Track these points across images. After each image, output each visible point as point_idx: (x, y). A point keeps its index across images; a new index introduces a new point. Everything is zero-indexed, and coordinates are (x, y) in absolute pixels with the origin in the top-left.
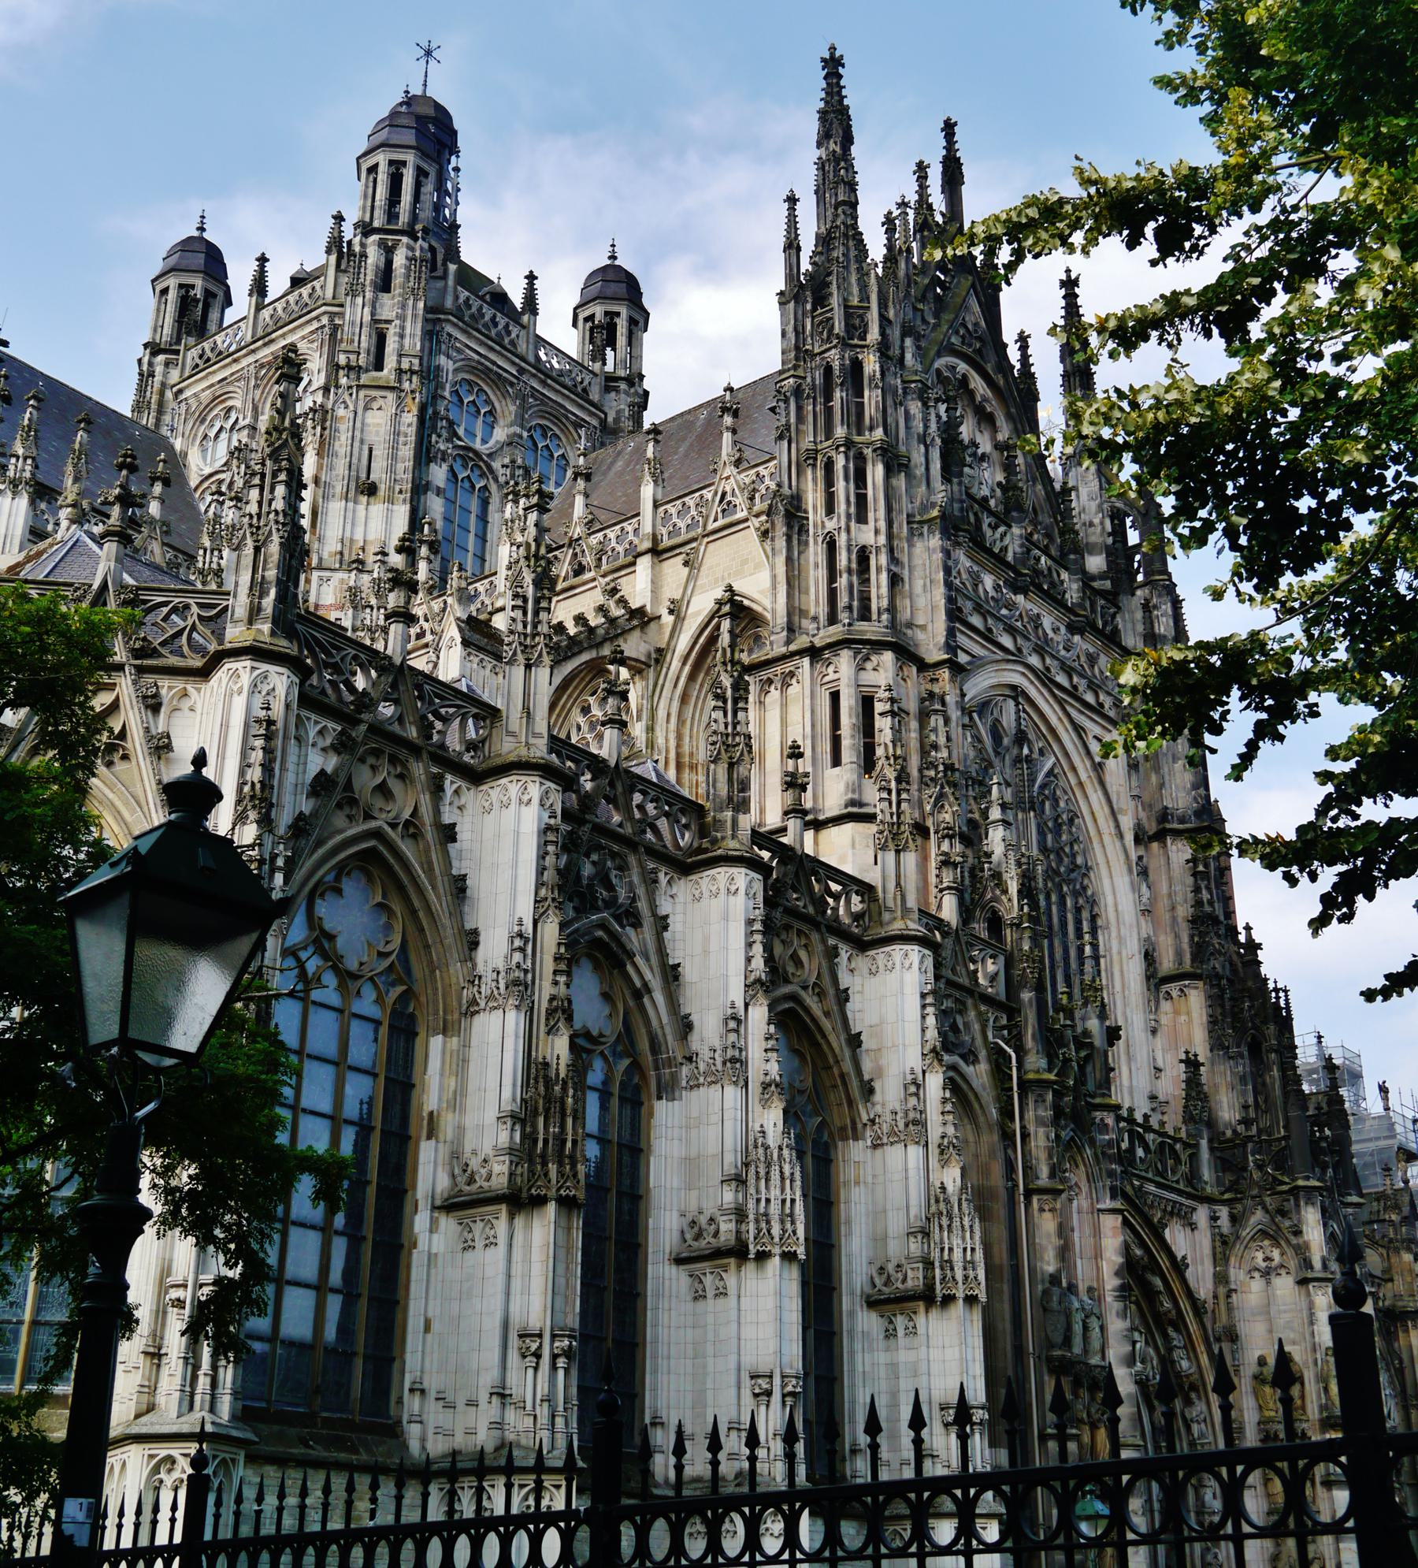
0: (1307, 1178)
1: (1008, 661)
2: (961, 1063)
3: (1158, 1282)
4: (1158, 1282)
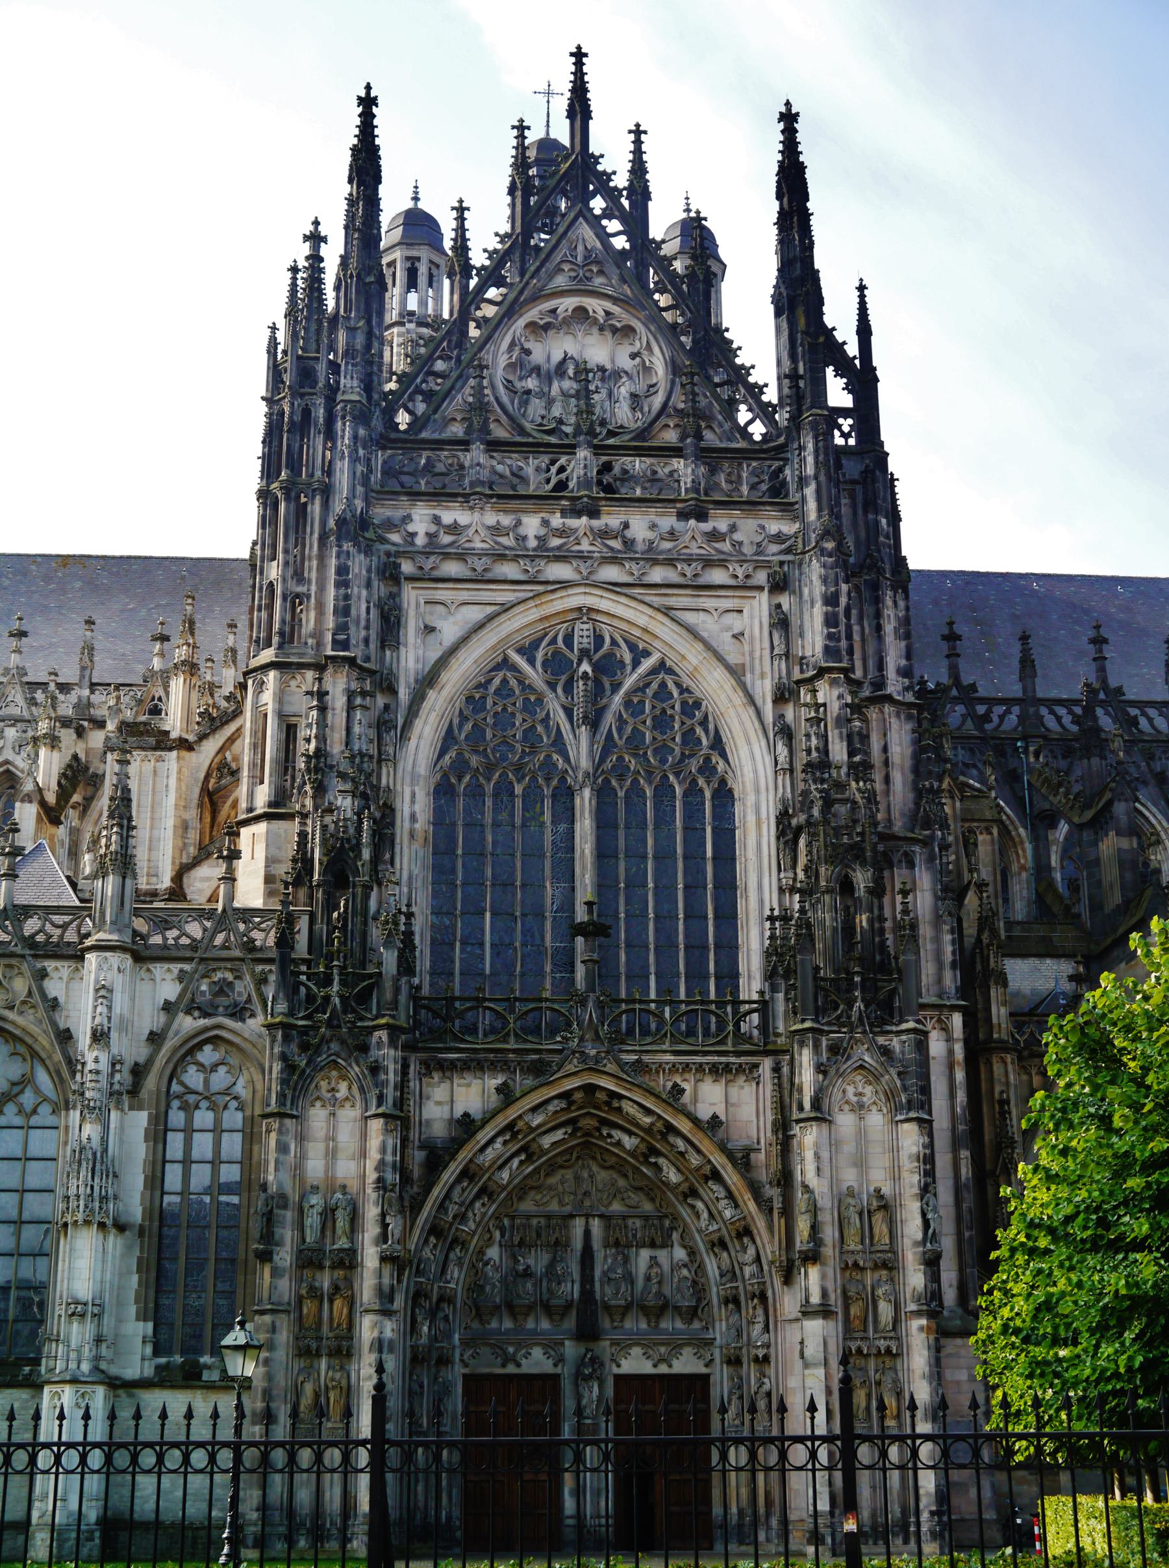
0: (803, 1021)
1: (553, 591)
2: (228, 1022)
3: (681, 1144)
4: (681, 1144)
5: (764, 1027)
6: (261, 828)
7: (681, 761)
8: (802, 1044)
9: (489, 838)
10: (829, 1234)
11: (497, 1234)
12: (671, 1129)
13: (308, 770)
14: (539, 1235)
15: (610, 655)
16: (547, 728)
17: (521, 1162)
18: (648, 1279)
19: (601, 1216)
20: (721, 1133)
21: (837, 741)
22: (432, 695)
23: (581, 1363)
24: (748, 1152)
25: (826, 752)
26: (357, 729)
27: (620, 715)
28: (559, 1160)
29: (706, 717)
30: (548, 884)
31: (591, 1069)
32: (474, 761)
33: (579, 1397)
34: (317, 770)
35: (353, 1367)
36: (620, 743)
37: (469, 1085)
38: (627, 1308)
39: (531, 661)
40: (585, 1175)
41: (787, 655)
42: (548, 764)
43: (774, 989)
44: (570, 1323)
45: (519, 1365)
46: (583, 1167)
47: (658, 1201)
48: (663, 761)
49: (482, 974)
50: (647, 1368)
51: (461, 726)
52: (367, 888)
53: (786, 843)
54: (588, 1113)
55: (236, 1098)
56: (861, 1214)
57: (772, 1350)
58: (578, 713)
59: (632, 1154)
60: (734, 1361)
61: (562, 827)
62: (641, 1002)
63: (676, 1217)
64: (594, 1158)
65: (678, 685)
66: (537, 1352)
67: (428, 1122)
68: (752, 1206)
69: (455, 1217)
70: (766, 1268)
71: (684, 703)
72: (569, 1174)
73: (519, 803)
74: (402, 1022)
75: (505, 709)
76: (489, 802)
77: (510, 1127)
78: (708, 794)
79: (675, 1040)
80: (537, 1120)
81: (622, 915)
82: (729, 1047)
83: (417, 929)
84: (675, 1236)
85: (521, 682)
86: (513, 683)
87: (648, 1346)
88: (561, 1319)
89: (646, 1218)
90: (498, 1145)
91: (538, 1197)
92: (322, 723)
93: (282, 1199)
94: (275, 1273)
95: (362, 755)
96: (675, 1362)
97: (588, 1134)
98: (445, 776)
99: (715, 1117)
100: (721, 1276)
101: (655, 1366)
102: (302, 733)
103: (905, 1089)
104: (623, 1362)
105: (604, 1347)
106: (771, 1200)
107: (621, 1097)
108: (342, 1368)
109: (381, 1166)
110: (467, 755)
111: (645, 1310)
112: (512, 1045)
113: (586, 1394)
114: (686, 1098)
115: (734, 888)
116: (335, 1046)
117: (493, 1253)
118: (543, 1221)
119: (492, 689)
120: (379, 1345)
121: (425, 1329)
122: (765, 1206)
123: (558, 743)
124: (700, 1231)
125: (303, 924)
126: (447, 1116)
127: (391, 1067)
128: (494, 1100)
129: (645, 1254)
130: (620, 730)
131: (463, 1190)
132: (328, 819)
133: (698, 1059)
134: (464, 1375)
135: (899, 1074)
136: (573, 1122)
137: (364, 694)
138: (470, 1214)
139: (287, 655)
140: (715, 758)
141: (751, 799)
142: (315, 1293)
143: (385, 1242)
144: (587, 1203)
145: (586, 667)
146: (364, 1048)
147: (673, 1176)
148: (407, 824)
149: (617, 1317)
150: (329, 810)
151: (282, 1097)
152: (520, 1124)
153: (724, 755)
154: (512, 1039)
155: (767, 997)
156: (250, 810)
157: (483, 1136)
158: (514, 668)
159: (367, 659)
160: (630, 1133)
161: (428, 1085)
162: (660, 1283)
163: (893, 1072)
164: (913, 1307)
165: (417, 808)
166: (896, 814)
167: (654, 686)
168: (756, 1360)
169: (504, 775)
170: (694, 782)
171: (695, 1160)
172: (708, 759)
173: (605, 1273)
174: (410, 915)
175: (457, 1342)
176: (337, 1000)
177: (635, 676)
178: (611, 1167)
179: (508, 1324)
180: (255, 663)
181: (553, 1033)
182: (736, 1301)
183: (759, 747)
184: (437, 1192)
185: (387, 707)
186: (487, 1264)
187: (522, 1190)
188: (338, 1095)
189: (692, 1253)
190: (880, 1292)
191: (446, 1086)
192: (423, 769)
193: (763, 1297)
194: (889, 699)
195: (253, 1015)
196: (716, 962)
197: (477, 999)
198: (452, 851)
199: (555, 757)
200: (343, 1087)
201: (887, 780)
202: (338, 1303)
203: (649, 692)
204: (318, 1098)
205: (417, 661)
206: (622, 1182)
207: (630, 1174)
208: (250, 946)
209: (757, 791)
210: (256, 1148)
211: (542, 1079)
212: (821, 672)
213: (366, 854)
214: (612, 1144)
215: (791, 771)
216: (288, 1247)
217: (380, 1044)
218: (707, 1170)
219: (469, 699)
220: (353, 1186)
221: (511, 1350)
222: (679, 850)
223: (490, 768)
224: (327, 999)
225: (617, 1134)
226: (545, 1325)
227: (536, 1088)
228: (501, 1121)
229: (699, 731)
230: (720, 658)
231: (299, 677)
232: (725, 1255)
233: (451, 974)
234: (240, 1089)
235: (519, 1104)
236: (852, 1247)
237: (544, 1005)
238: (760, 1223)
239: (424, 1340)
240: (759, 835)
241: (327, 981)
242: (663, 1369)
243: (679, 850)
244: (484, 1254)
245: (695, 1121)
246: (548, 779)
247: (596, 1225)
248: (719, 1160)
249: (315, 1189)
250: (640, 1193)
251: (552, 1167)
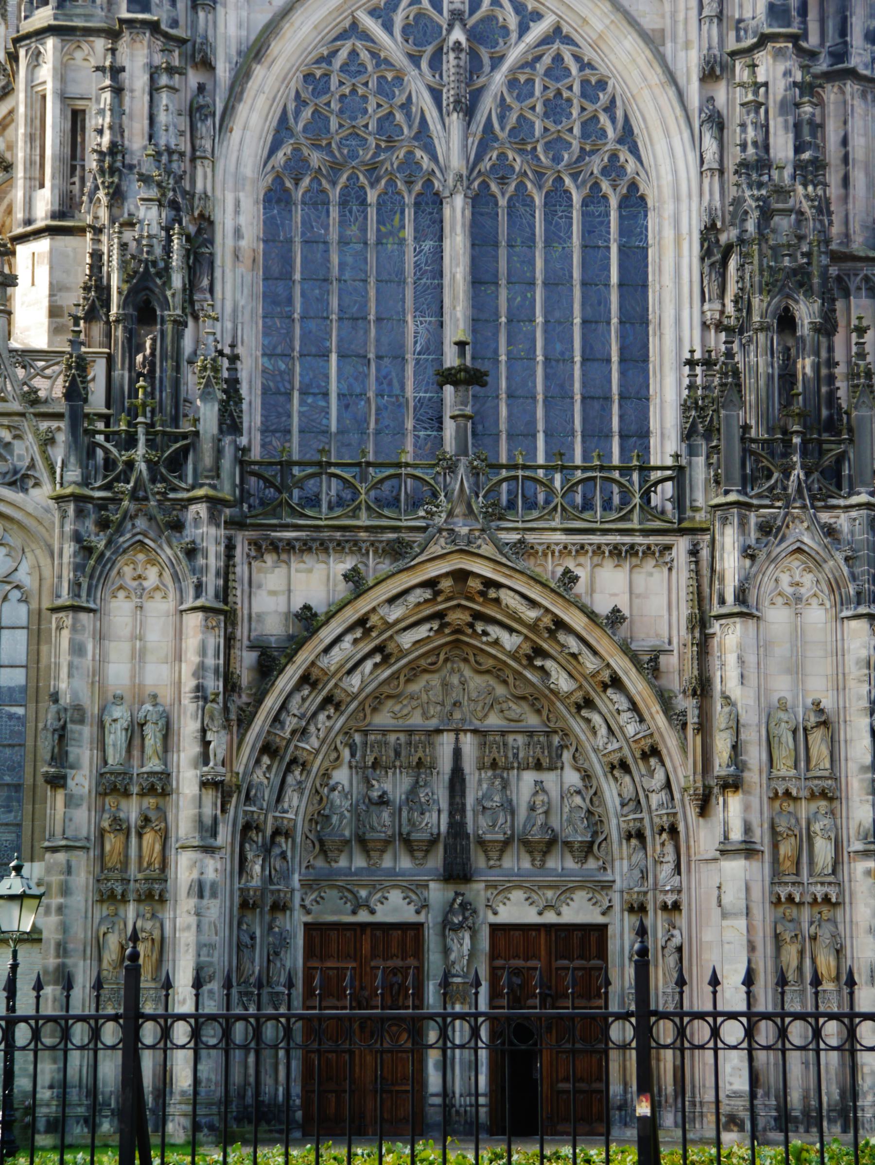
0: (727, 492)
3: (573, 645)
4: (573, 645)
5: (679, 500)
6: (43, 245)
7: (580, 159)
8: (725, 521)
9: (335, 259)
10: (755, 756)
11: (346, 753)
12: (560, 624)
13: (102, 171)
14: (397, 754)
15: (490, 18)
16: (408, 115)
17: (376, 665)
18: (532, 808)
19: (475, 731)
20: (623, 630)
21: (781, 132)
22: (259, 71)
23: (449, 910)
24: (656, 655)
25: (767, 148)
26: (162, 118)
27: (503, 99)
28: (423, 663)
29: (613, 101)
30: (409, 318)
31: (462, 551)
32: (316, 158)
33: (446, 951)
34: (112, 171)
35: (167, 915)
36: (502, 135)
37: (310, 571)
38: (506, 844)
39: (388, 27)
40: (455, 680)
41: (720, 17)
42: (410, 164)
43: (692, 452)
44: (436, 861)
45: (373, 912)
46: (453, 671)
47: (545, 713)
48: (557, 159)
49: (326, 432)
50: (530, 916)
51: (297, 113)
52: (180, 324)
53: (712, 265)
54: (459, 606)
55: (17, 587)
56: (795, 732)
57: (684, 896)
58: (448, 96)
59: (514, 656)
60: (638, 909)
61: (428, 245)
62: (525, 467)
63: (566, 733)
64: (466, 660)
65: (577, 58)
66: (395, 897)
67: (259, 615)
68: (661, 720)
69: (293, 732)
70: (677, 796)
71: (585, 83)
72: (435, 680)
73: (372, 213)
74: (226, 492)
75: (354, 91)
76: (334, 213)
77: (362, 622)
78: (614, 202)
79: (566, 515)
80: (395, 613)
81: (503, 358)
82: (635, 524)
83: (243, 375)
84: (567, 756)
85: (374, 55)
86: (364, 56)
87: (531, 888)
88: (425, 857)
89: (531, 734)
90: (347, 643)
91: (397, 708)
92: (118, 110)
93: (79, 713)
94: (70, 801)
95: (170, 152)
96: (564, 909)
97: (458, 631)
98: (278, 179)
99: (616, 611)
100: (623, 805)
101: (540, 913)
102: (93, 121)
103: (854, 577)
104: (501, 909)
105: (477, 891)
106: (684, 713)
107: (498, 586)
108: (153, 916)
109: (200, 670)
110: (306, 151)
111: (528, 845)
112: (364, 520)
113: (455, 947)
114: (580, 588)
115: (645, 322)
116: (141, 523)
117: (341, 776)
118: (403, 737)
119: (338, 62)
120: (200, 889)
121: (257, 868)
122: (679, 722)
123: (423, 134)
124: (596, 750)
125: (98, 370)
126: (283, 608)
127: (212, 550)
128: (342, 589)
129: (529, 777)
130: (502, 118)
131: (304, 700)
132: (129, 235)
133: (596, 539)
134: (306, 925)
135: (847, 559)
136: (439, 616)
137: (171, 70)
138: (312, 729)
139: (70, 17)
140: (624, 155)
141: (669, 209)
142: (119, 826)
143: (206, 763)
144: (457, 715)
145: (458, 35)
146: (178, 526)
147: (563, 683)
148: (230, 242)
149: (494, 855)
150: (131, 225)
151: (76, 586)
152: (374, 620)
153: (634, 151)
154: (364, 514)
155: (683, 462)
156: (28, 222)
157: (327, 634)
158: (366, 36)
159: (175, 23)
160: (511, 630)
161: (260, 570)
162: (547, 813)
163: (839, 557)
164: (858, 846)
165: (243, 220)
166: (855, 226)
167: (547, 60)
168: (665, 907)
169: (353, 177)
170: (596, 186)
171: (590, 663)
172: (614, 157)
173: (479, 801)
174: (234, 359)
175: (296, 884)
176: (142, 466)
177: (522, 47)
178: (488, 672)
179: (359, 862)
180: (28, 26)
181: (416, 504)
182: (640, 836)
183: (681, 140)
184: (271, 702)
185: (201, 88)
186: (333, 789)
187: (377, 700)
188: (146, 584)
189: (587, 776)
190: (816, 827)
191: (282, 570)
192: (249, 168)
193: (673, 831)
194: (852, 74)
195: (37, 484)
196: (621, 417)
197: (319, 464)
198: (286, 276)
199: (419, 153)
200: (152, 574)
201: (846, 181)
202: (149, 837)
203: (541, 67)
204: (121, 588)
205: (240, 26)
206: (500, 691)
207: (511, 680)
208: (32, 398)
209: (677, 198)
210: (44, 648)
211: (401, 564)
212: (764, 40)
213: (177, 281)
214: (488, 643)
215: (721, 172)
216: (86, 770)
217: (197, 521)
218: (606, 676)
219: (308, 77)
220: (166, 696)
221: (363, 893)
222: (577, 274)
223: (336, 168)
224: (130, 464)
225: (495, 631)
226: (405, 863)
227: (393, 575)
228: (350, 615)
229: (604, 119)
230: (632, 22)
231: (85, 46)
232: (627, 779)
233: (289, 432)
234: (23, 576)
235: (372, 594)
236: (783, 772)
237: (403, 471)
238: (670, 742)
239: (256, 882)
240: (678, 255)
241: (130, 442)
242: (550, 918)
243: (577, 274)
244: (329, 777)
245: (591, 615)
246: (409, 183)
247: (468, 743)
248: (621, 664)
249: (119, 699)
250: (523, 704)
251: (414, 671)
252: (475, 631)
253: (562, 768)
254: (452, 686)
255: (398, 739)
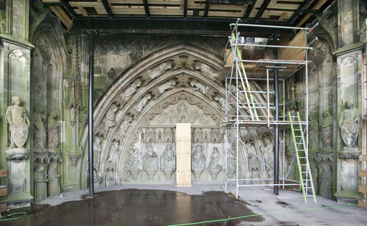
14: (160, 137)
40: (182, 108)
54: (183, 73)
72: (174, 107)
80: (154, 74)
84: (225, 138)
91: (160, 119)
129: (211, 146)
206: (200, 111)
225: (199, 85)
252: (190, 85)
253: (224, 142)
254: (181, 110)
255: (160, 131)
